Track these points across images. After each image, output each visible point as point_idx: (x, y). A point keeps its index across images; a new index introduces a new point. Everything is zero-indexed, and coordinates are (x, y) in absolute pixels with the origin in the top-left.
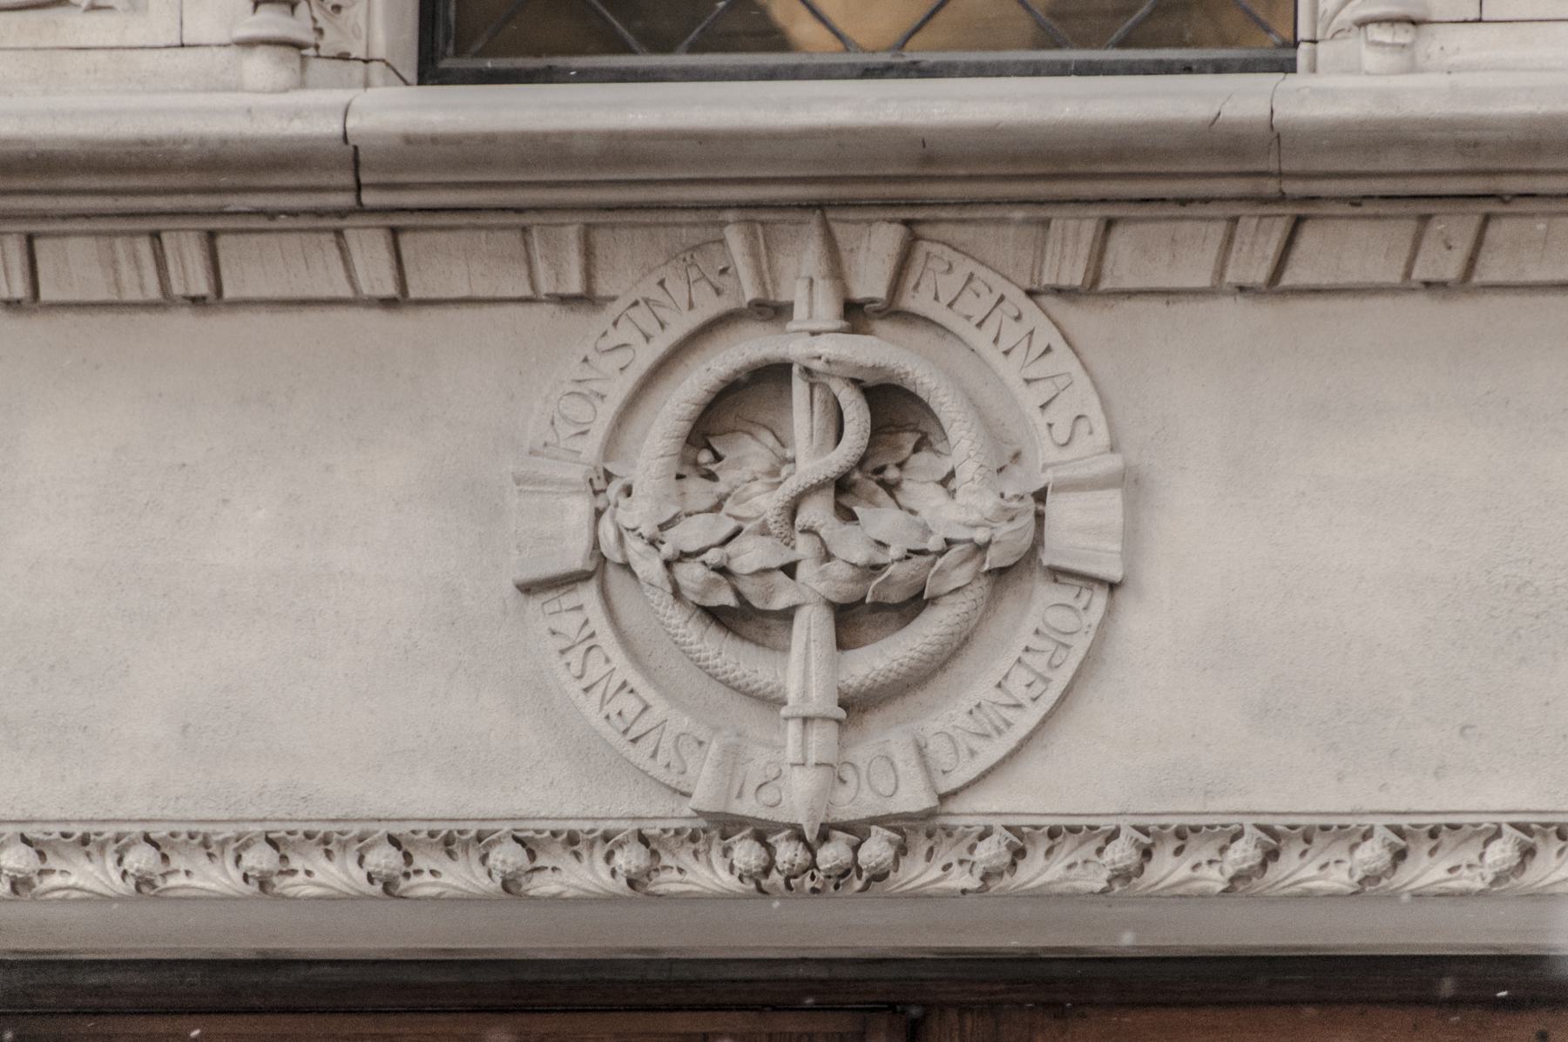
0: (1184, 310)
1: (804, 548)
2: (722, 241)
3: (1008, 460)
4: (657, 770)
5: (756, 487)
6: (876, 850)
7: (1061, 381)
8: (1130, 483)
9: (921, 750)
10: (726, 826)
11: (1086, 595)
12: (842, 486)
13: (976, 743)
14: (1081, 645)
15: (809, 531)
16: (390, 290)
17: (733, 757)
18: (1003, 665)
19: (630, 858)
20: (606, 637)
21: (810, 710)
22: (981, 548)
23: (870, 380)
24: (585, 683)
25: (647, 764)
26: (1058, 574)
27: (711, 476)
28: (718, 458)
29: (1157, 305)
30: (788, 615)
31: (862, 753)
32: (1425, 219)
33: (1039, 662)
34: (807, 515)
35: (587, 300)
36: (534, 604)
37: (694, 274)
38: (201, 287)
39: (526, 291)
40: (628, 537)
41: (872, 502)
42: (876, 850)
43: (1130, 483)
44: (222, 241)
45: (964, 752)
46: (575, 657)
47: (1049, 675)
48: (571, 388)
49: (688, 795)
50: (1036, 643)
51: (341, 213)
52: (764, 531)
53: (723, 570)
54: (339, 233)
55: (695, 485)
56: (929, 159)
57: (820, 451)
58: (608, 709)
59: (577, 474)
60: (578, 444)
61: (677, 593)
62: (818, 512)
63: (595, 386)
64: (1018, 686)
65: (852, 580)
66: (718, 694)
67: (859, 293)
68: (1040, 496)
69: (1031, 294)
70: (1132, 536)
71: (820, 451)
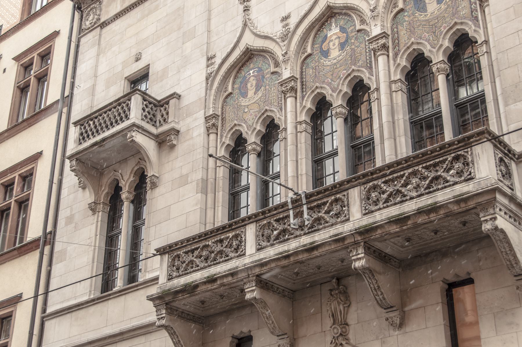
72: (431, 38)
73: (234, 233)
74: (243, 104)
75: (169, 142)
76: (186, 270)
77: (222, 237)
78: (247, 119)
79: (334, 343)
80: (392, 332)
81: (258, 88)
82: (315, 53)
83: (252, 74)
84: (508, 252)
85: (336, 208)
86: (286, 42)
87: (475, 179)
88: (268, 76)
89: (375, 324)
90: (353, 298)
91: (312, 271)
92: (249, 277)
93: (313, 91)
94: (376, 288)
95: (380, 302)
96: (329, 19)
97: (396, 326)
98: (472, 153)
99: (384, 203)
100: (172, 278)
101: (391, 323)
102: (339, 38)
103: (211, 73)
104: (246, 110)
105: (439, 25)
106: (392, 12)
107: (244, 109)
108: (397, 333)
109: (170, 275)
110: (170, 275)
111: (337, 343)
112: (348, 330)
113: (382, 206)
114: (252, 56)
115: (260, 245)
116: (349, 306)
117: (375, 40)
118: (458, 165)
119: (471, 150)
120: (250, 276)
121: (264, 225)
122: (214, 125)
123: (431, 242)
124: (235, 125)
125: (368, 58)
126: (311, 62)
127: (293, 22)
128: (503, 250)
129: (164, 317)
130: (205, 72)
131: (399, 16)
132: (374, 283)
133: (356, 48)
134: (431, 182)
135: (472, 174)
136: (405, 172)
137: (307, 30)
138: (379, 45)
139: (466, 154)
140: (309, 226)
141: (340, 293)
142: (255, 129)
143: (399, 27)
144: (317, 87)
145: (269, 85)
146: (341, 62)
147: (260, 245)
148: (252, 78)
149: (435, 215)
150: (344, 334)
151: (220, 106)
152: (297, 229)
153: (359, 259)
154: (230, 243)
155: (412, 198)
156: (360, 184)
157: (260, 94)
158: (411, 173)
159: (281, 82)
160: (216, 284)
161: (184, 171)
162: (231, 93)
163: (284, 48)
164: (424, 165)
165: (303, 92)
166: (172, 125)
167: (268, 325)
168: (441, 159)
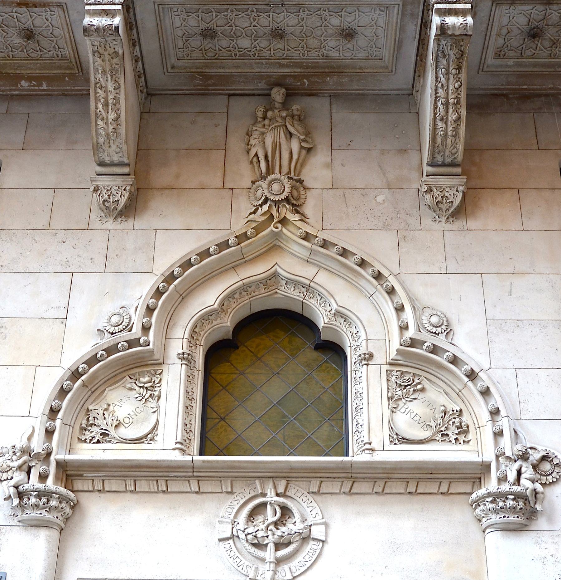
0: (334, 496)
1: (270, 533)
2: (255, 483)
3: (304, 520)
4: (243, 572)
5: (260, 524)
7: (314, 507)
8: (326, 525)
9: (290, 569)
11: (319, 543)
12: (276, 524)
13: (300, 568)
14: (318, 551)
15: (271, 530)
16: (197, 490)
17: (257, 569)
18: (304, 554)
20: (234, 548)
21: (271, 560)
22: (301, 534)
23: (282, 505)
24: (230, 556)
25: (241, 571)
26: (314, 539)
27: (253, 522)
28: (254, 519)
29: (329, 495)
30: (266, 545)
31: (280, 569)
32: (375, 482)
33: (311, 554)
34: (270, 528)
35: (231, 493)
36: (221, 543)
37: (250, 488)
38: (165, 489)
39: (221, 491)
40: (238, 531)
41: (281, 526)
43: (326, 525)
44: (168, 482)
45: (298, 570)
46: (229, 552)
47: (312, 556)
48: (228, 507)
49: (248, 576)
50: (310, 551)
51: (189, 477)
52: (262, 530)
53: (256, 537)
54: (189, 481)
55: (250, 523)
56: (292, 469)
57: (273, 517)
58: (234, 561)
59: (230, 521)
60: (229, 516)
61: (247, 541)
62: (272, 527)
63: (233, 506)
64: (307, 558)
65: (278, 539)
66: (253, 559)
67: (279, 492)
68: (310, 526)
69: (308, 493)
70: (326, 534)
71: (273, 517)
79: (265, 213)
80: (427, 222)
91: (245, 43)
94: (451, 101)
95: (439, 140)
97: (448, 210)
101: (439, 199)
112: (303, 196)
116: (309, 150)
132: (451, 87)
141: (293, 116)
150: (295, 202)
167: (100, 122)
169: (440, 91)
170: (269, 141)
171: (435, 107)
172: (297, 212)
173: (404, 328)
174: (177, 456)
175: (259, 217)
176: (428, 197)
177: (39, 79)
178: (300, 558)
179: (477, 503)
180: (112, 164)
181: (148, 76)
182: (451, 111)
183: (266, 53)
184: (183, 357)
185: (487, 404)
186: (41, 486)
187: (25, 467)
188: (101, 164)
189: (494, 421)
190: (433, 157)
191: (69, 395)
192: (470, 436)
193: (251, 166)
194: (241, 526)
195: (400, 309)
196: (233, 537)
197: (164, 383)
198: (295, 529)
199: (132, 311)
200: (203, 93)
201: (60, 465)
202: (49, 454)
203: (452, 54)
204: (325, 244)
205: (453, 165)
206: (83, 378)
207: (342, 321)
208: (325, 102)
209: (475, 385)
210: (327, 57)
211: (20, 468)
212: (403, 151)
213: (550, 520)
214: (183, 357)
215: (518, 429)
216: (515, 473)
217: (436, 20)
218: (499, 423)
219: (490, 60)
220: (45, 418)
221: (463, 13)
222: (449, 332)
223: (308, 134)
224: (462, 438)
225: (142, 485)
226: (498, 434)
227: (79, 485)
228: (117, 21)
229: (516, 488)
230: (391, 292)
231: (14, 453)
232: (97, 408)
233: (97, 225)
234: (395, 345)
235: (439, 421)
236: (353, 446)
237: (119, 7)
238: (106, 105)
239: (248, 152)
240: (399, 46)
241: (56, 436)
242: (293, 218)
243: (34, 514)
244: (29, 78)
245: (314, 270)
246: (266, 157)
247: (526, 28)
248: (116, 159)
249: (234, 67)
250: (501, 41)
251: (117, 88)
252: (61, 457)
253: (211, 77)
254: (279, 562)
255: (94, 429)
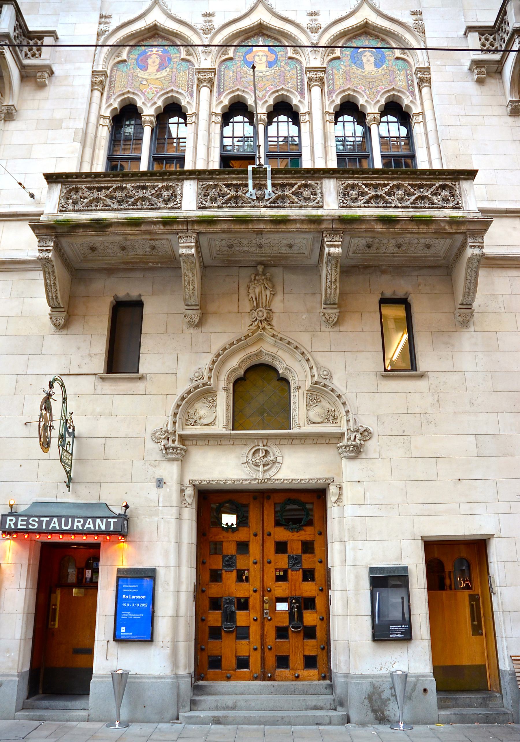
3: (274, 455)
6: (266, 481)
8: (282, 457)
10: (256, 479)
12: (263, 457)
17: (256, 474)
19: (249, 481)
35: (246, 445)
42: (266, 481)
43: (282, 457)
62: (262, 458)
72: (368, 92)
73: (165, 184)
74: (139, 75)
75: (39, 79)
76: (88, 207)
77: (147, 184)
78: (145, 91)
79: (256, 326)
80: (323, 328)
81: (161, 67)
82: (237, 59)
83: (154, 52)
84: (473, 281)
85: (306, 193)
86: (209, 36)
87: (462, 210)
88: (176, 60)
89: (304, 317)
90: (279, 288)
91: (246, 249)
92: (187, 232)
93: (233, 92)
94: (333, 280)
95: (328, 295)
96: (256, 36)
98: (459, 188)
99: (365, 203)
100: (66, 211)
101: (328, 319)
102: (267, 56)
103: (105, 31)
104: (144, 82)
105: (377, 84)
106: (328, 55)
107: (142, 81)
108: (330, 329)
109: (63, 207)
110: (63, 207)
111: (259, 327)
113: (363, 205)
114: (157, 36)
115: (202, 204)
116: (274, 294)
117: (314, 71)
118: (445, 193)
119: (459, 184)
120: (189, 231)
121: (209, 186)
122: (101, 82)
123: (382, 257)
124: (129, 92)
125: (299, 84)
126: (232, 65)
127: (218, 22)
128: (469, 278)
129: (50, 250)
130: (97, 28)
131: (333, 62)
132: (333, 275)
133: (285, 72)
134: (417, 199)
135: (460, 205)
136: (390, 182)
137: (233, 35)
138: (317, 76)
139: (453, 186)
140: (271, 200)
141: (267, 279)
142: (155, 103)
143: (334, 70)
144: (238, 90)
145: (176, 69)
146: (268, 77)
147: (202, 204)
148: (154, 56)
149: (426, 228)
151: (109, 68)
152: (253, 200)
153: (335, 246)
154: (157, 193)
155: (396, 207)
156: (337, 178)
157: (164, 73)
158: (396, 185)
159: (200, 69)
160: (138, 229)
161: (58, 115)
162: (125, 61)
163: (207, 40)
164: (410, 183)
165: (219, 88)
166: (47, 62)
167: (186, 290)
168: (428, 183)
169: (328, 276)
170: (257, 291)
171: (327, 283)
172: (270, 324)
173: (313, 376)
174: (224, 431)
175: (253, 327)
176: (324, 318)
177: (157, 263)
178: (273, 470)
179: (340, 448)
180: (192, 305)
181: (203, 257)
182: (333, 284)
183: (255, 252)
184: (224, 389)
185: (345, 408)
186: (174, 445)
187: (167, 438)
188: (187, 305)
189: (347, 415)
190: (326, 302)
191: (181, 407)
192: (338, 420)
193: (249, 302)
194: (250, 458)
195: (311, 368)
196: (247, 462)
197: (218, 400)
198: (270, 459)
199: (203, 370)
200: (228, 267)
201: (180, 436)
202: (175, 432)
203: (333, 262)
204: (281, 339)
205: (334, 304)
206: (186, 400)
207: (288, 371)
208: (281, 269)
209: (340, 400)
210: (282, 253)
211: (165, 438)
212: (314, 294)
213: (366, 454)
214: (224, 389)
215: (356, 418)
216: (354, 437)
217: (327, 250)
218: (349, 416)
219: (351, 254)
220: (172, 417)
221: (338, 246)
222: (331, 378)
223: (273, 287)
224: (335, 421)
225: (211, 442)
226: (348, 421)
227: (187, 442)
228: (193, 251)
229: (354, 443)
230: (308, 360)
231: (162, 432)
232: (192, 411)
233: (186, 331)
234: (309, 383)
235: (326, 414)
236: (293, 425)
237: (193, 244)
238: (189, 283)
239: (248, 295)
240: (312, 251)
241: (177, 424)
242: (268, 327)
243: (171, 456)
244: (153, 262)
245: (276, 349)
246: (256, 298)
247: (366, 244)
248: (193, 303)
249: (242, 257)
250: (355, 248)
251: (193, 276)
252: (180, 433)
253: (231, 261)
254: (265, 471)
255: (191, 420)
